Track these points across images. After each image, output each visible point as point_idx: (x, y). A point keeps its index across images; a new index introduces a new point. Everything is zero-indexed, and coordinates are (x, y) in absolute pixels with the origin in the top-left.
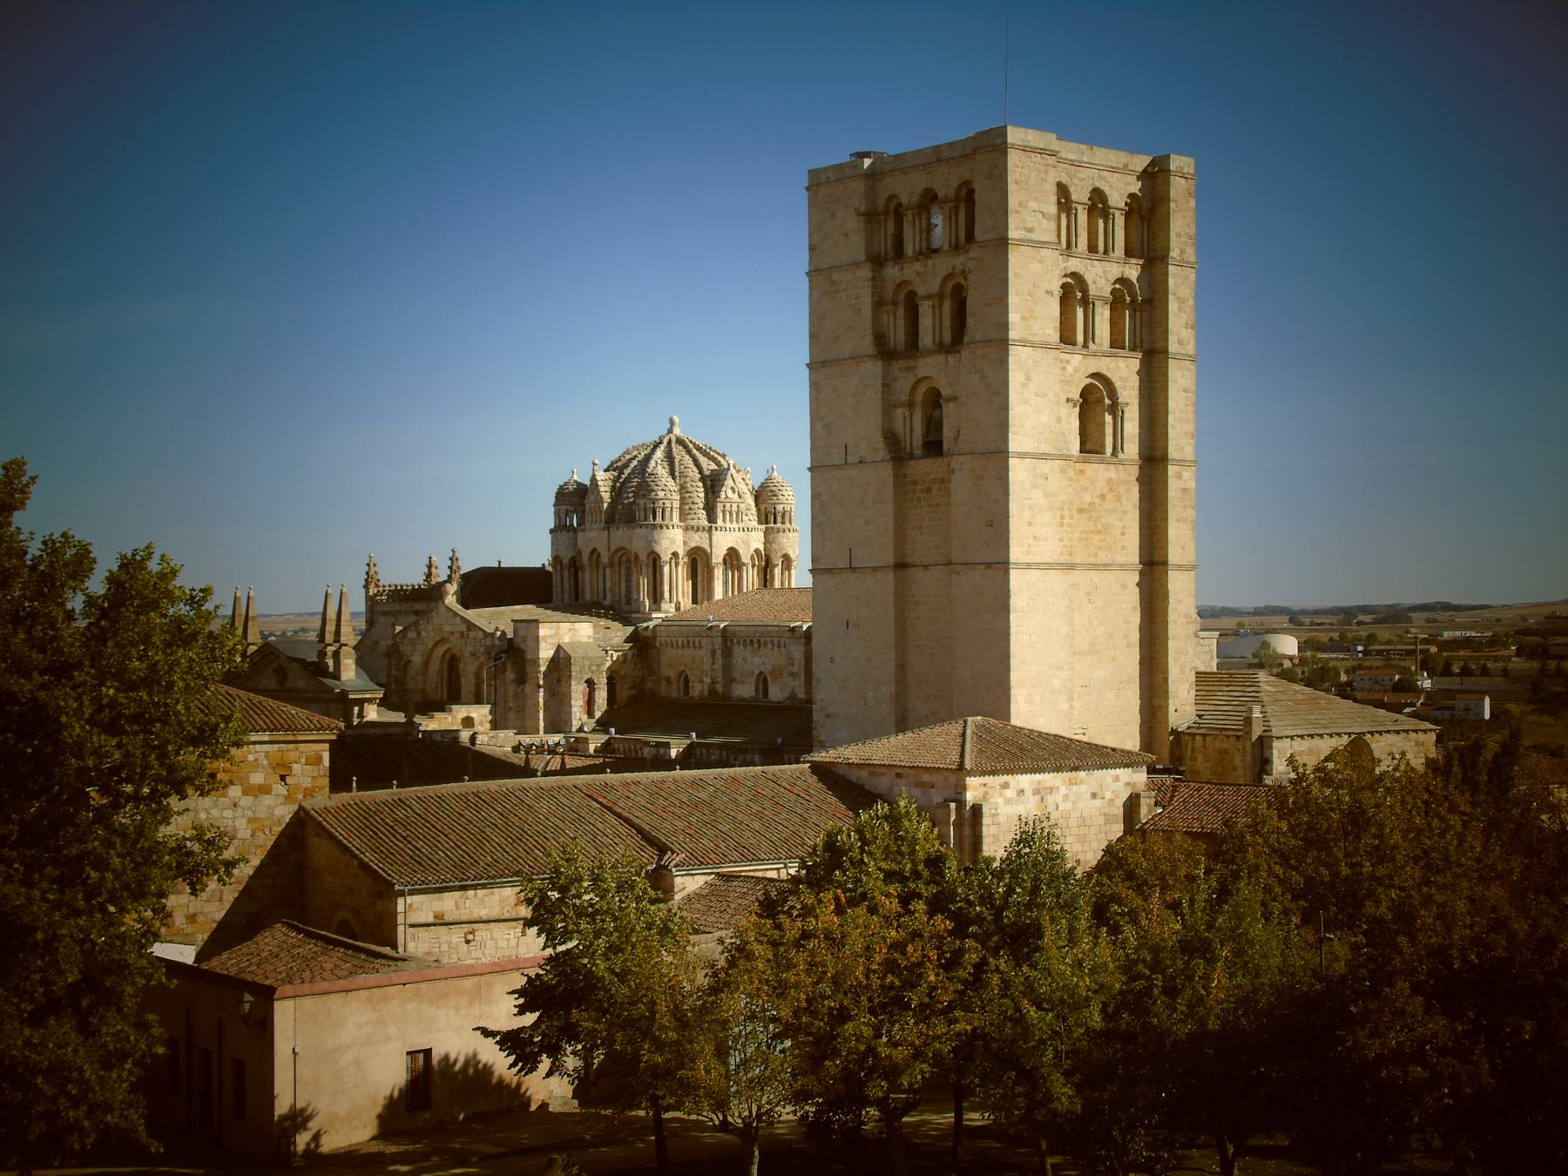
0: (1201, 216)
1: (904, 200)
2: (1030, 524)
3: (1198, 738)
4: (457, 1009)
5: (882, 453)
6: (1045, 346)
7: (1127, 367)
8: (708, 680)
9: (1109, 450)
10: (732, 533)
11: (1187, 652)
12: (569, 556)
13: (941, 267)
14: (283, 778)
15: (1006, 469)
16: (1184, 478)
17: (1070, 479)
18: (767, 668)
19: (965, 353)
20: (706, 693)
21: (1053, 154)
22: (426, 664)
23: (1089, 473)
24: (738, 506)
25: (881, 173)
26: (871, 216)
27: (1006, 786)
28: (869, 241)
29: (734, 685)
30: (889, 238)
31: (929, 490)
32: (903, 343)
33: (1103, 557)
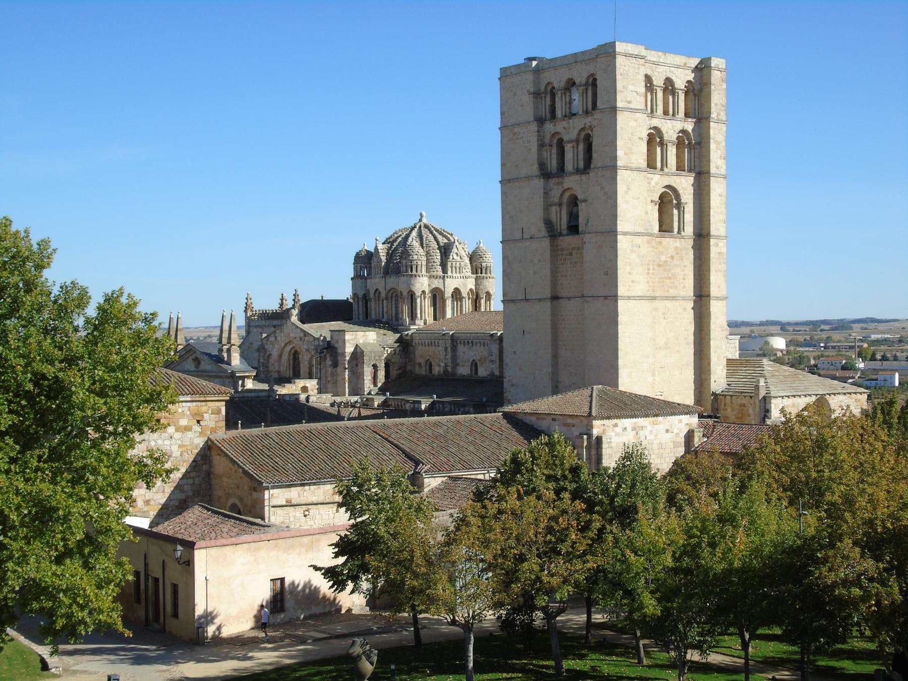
0: (729, 93)
1: (556, 86)
2: (630, 273)
3: (728, 397)
4: (300, 554)
5: (544, 232)
6: (638, 170)
7: (686, 181)
8: (443, 364)
9: (676, 230)
10: (457, 280)
12: (362, 294)
13: (578, 123)
14: (198, 422)
15: (616, 241)
17: (653, 247)
18: (477, 358)
19: (592, 174)
20: (442, 372)
21: (643, 58)
22: (280, 356)
24: (460, 264)
25: (542, 70)
26: (536, 94)
27: (616, 425)
28: (536, 109)
29: (458, 367)
30: (547, 108)
31: (571, 254)
32: (556, 168)
33: (672, 292)
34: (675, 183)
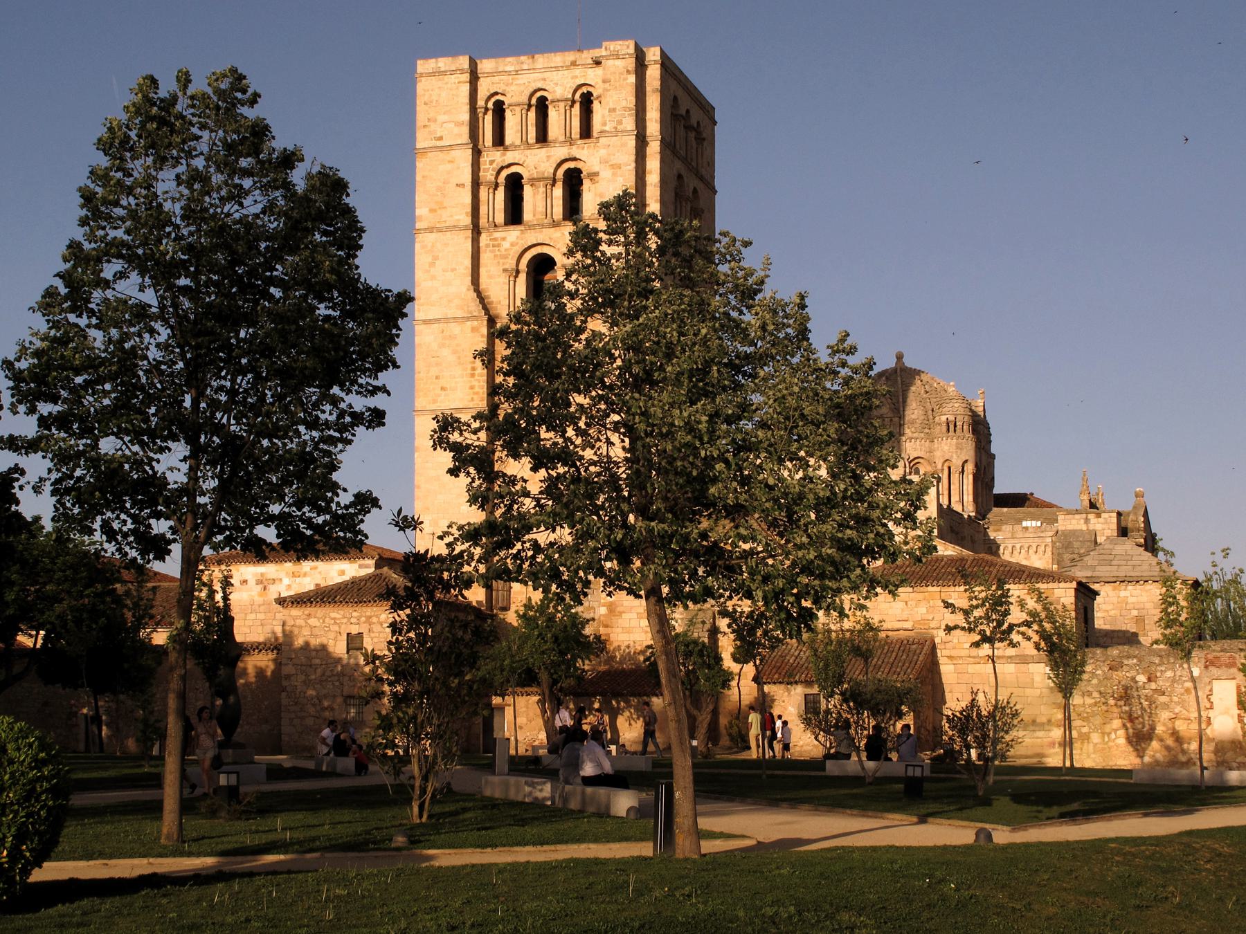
2: (437, 378)
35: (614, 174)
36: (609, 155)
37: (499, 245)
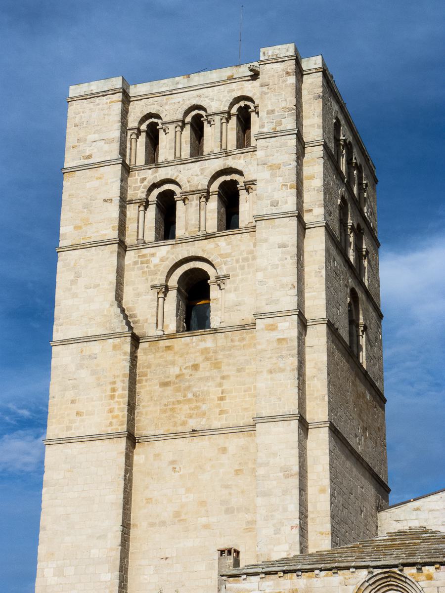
2: (73, 402)
7: (228, 244)
11: (285, 510)
16: (279, 328)
23: (176, 348)
33: (193, 424)
34: (203, 250)
35: (272, 175)
36: (267, 156)
37: (148, 262)
